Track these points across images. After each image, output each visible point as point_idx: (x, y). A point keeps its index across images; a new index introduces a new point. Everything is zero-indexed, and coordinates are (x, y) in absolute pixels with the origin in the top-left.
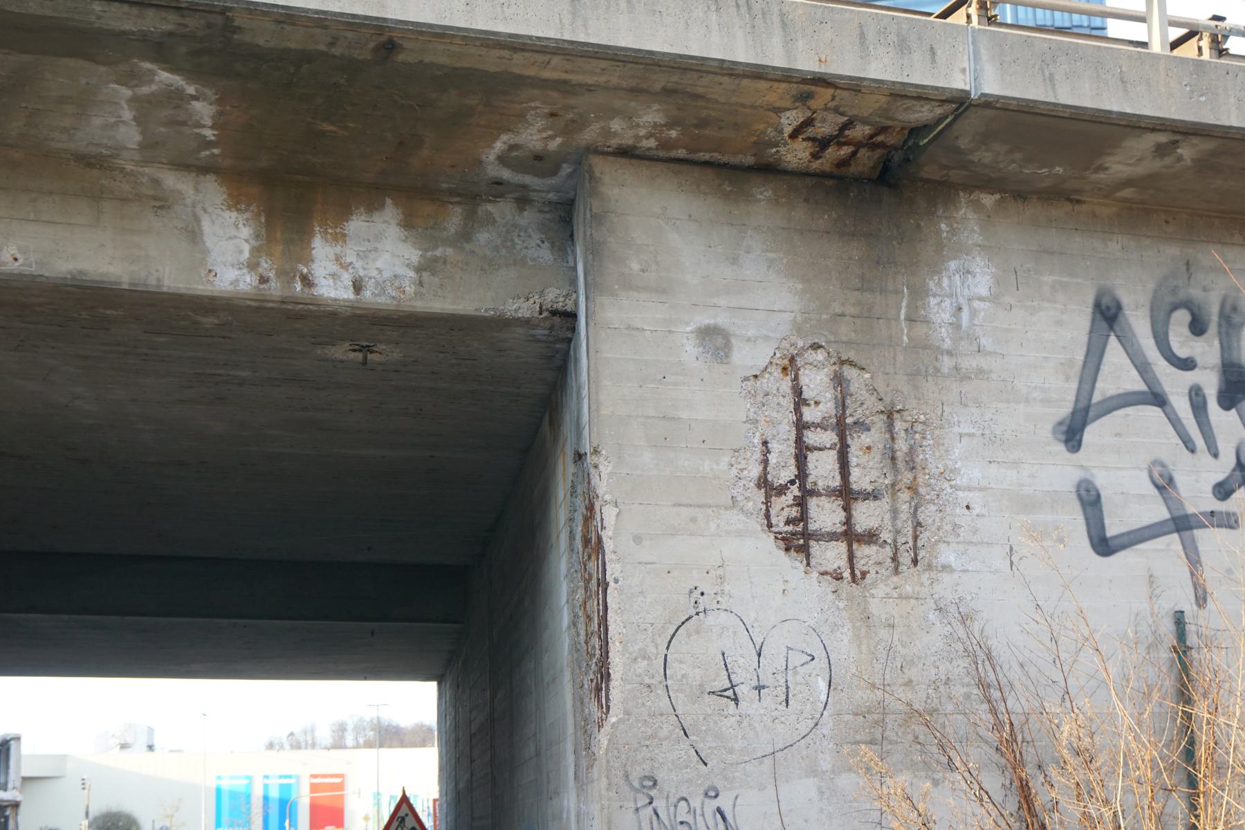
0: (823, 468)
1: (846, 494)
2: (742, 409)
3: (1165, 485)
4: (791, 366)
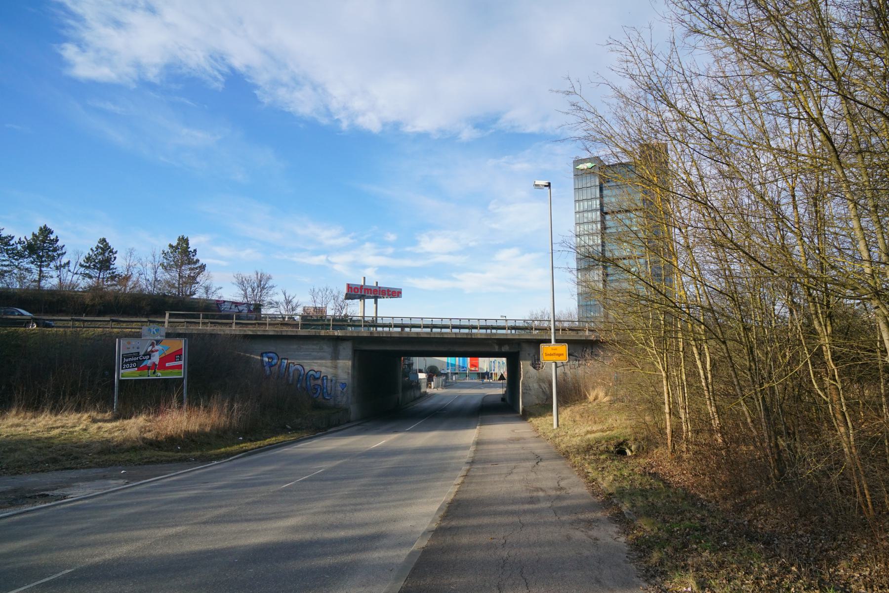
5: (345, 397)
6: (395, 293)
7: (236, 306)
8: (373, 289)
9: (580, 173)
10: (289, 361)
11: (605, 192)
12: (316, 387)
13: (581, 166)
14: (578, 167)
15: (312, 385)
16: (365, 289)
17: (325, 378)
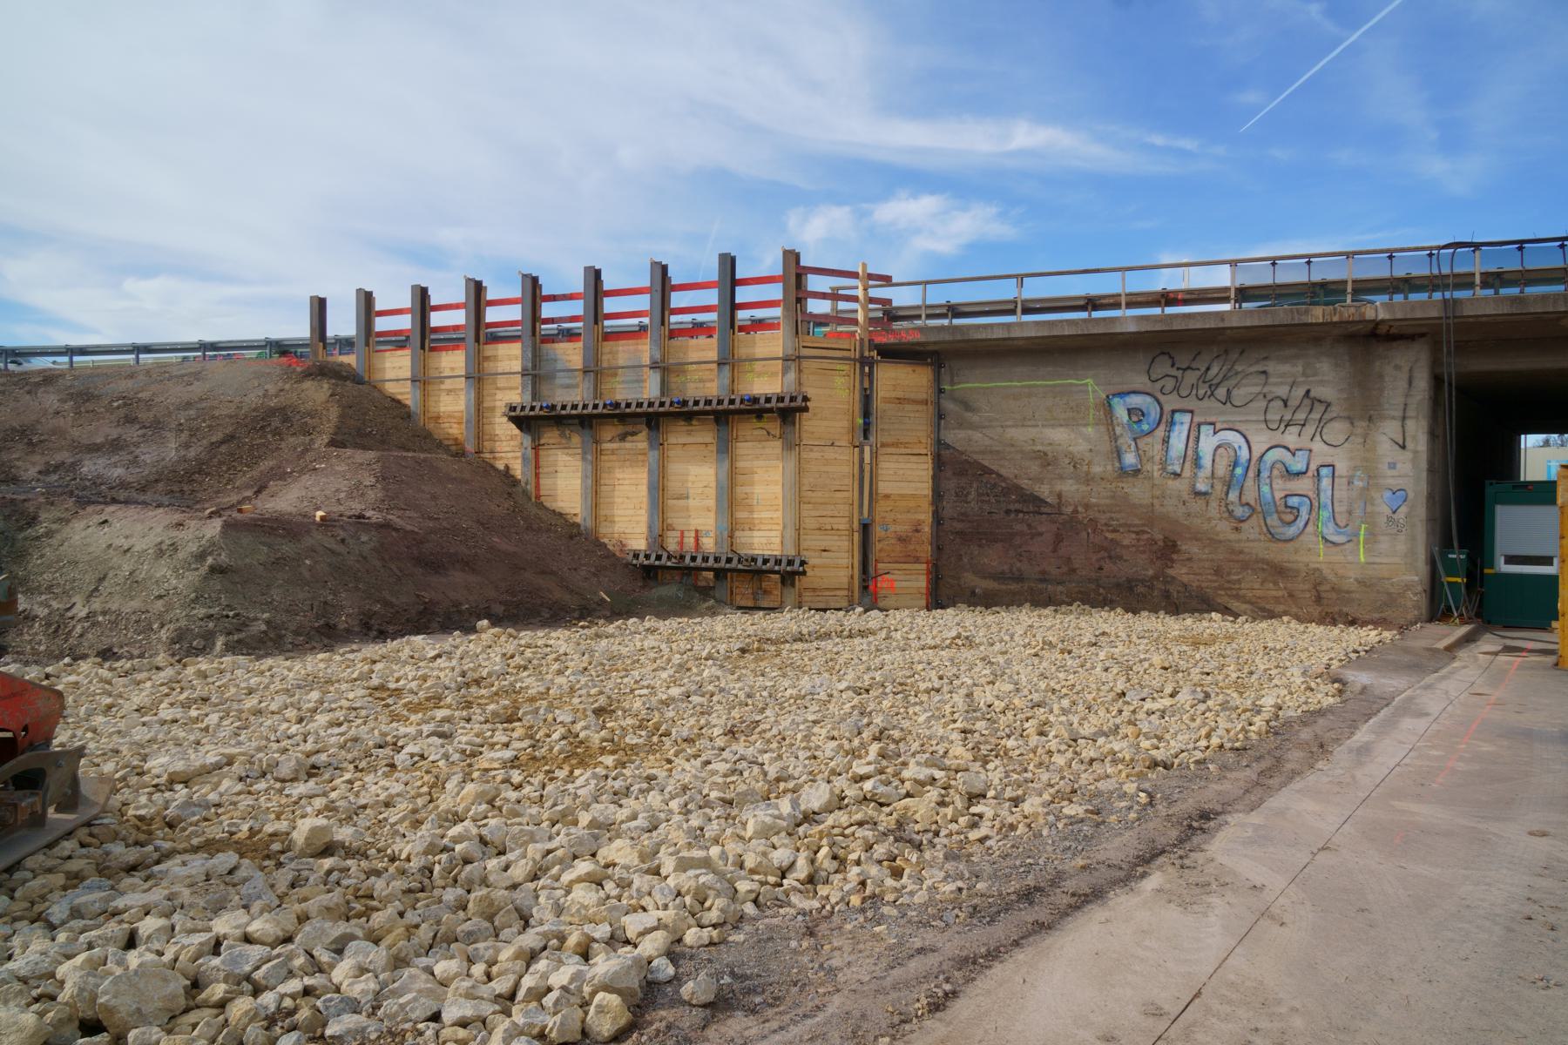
5: (1402, 537)
10: (1197, 419)
12: (1294, 501)
15: (1279, 495)
17: (1324, 471)
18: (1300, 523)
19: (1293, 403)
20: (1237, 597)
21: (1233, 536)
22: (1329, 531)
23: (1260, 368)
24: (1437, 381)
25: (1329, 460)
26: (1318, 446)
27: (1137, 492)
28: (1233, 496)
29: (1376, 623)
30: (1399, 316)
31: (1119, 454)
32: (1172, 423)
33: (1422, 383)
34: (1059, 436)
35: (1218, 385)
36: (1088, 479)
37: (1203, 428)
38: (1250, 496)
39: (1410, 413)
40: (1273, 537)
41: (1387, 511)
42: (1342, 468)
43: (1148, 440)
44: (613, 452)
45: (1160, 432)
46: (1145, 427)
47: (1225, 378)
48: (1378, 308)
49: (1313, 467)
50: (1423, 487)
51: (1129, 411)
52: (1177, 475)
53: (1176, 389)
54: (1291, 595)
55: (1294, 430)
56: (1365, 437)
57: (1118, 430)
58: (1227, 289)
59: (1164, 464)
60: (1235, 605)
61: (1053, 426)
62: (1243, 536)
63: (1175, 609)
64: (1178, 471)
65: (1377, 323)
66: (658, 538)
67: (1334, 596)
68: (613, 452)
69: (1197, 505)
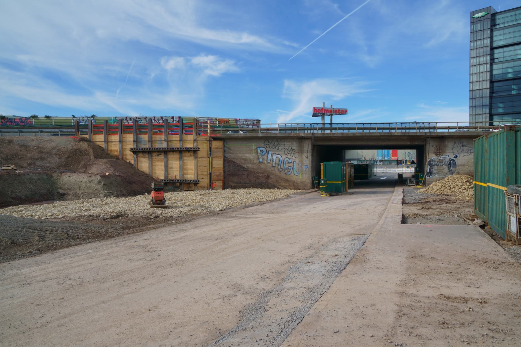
0: (438, 151)
1: (439, 153)
2: (434, 149)
3: (458, 151)
4: (437, 147)
6: (344, 112)
7: (246, 122)
8: (329, 110)
9: (475, 20)
10: (273, 153)
11: (495, 33)
12: (289, 168)
13: (476, 16)
14: (474, 17)
15: (287, 167)
16: (325, 110)
17: (294, 162)
18: (291, 172)
19: (289, 150)
20: (280, 185)
21: (279, 174)
22: (295, 173)
23: (284, 143)
24: (312, 145)
25: (295, 160)
26: (293, 158)
27: (262, 166)
28: (279, 167)
29: (302, 189)
30: (306, 135)
31: (259, 159)
32: (268, 153)
33: (310, 147)
34: (248, 155)
35: (276, 146)
36: (253, 164)
37: (274, 154)
38: (282, 167)
39: (308, 152)
40: (286, 174)
41: (305, 169)
42: (297, 162)
43: (264, 156)
44: (156, 158)
45: (266, 155)
46: (264, 154)
47: (277, 145)
48: (302, 134)
49: (293, 162)
50: (310, 165)
51: (261, 151)
52: (269, 163)
53: (269, 147)
54: (289, 185)
55: (289, 155)
56: (301, 156)
57: (259, 154)
58: (277, 128)
59: (267, 161)
60: (280, 187)
61: (247, 153)
62: (281, 174)
63: (269, 188)
64: (269, 162)
65: (302, 137)
66: (166, 176)
67: (296, 185)
68: (156, 158)
69: (273, 169)
